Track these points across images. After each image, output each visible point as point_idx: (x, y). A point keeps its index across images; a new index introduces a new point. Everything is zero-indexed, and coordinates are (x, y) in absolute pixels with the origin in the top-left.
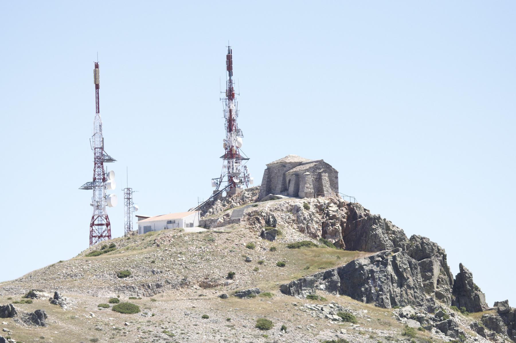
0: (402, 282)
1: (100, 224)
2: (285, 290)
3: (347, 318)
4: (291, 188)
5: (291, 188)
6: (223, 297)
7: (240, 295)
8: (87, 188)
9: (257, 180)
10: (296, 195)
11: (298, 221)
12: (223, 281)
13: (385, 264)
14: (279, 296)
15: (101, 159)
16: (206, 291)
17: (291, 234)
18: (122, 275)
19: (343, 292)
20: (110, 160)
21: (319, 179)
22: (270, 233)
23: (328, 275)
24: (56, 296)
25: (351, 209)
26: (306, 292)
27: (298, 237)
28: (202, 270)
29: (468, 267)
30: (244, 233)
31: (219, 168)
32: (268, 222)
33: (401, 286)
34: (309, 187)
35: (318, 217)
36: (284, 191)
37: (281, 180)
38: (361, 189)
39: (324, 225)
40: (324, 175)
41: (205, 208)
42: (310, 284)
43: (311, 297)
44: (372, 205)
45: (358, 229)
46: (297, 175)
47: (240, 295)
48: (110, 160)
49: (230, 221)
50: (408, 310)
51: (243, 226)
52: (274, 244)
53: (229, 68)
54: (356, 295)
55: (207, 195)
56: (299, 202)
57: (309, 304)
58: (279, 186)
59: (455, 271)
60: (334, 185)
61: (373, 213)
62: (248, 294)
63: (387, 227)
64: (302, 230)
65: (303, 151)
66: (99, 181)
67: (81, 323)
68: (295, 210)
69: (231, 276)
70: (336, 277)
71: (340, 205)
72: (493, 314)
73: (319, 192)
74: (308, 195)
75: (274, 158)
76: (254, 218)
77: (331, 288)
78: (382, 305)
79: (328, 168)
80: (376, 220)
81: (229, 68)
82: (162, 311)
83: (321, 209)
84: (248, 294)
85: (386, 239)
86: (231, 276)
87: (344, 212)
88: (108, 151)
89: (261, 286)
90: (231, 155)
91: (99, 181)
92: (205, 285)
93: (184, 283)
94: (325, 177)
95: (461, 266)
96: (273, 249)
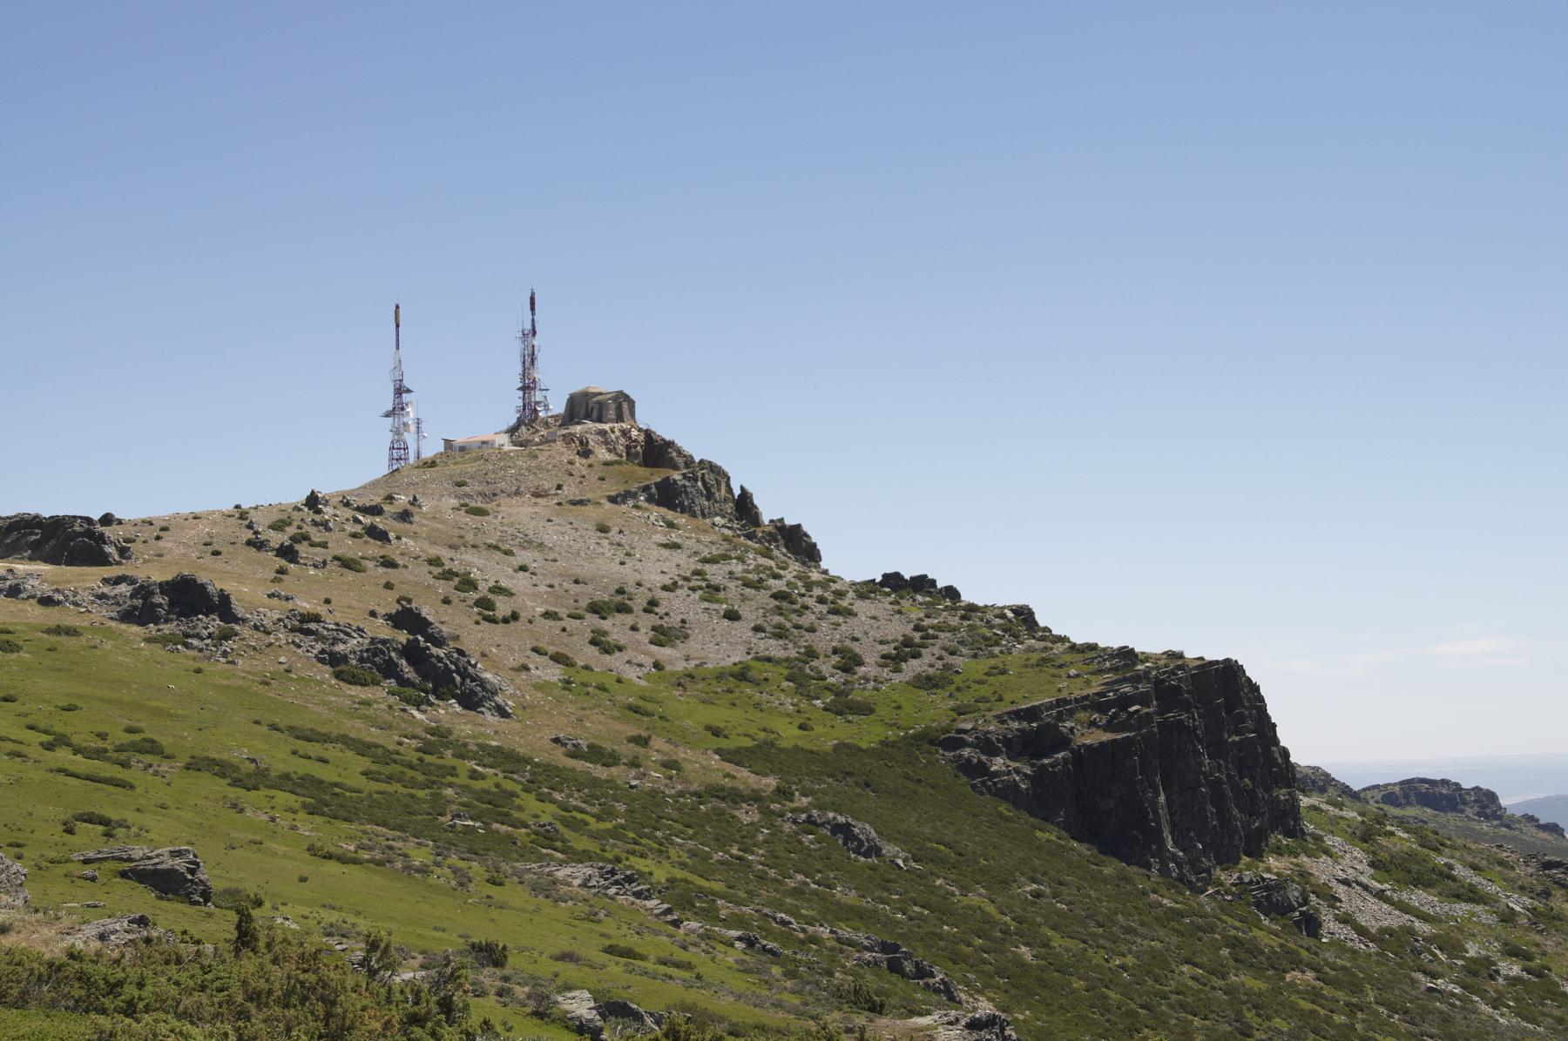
0: (710, 496)
1: (398, 449)
2: (612, 500)
3: (671, 525)
4: (595, 414)
5: (595, 414)
6: (559, 504)
7: (574, 503)
8: (387, 416)
9: (558, 406)
10: (600, 420)
11: (606, 443)
12: (553, 491)
13: (696, 480)
14: (608, 505)
15: (400, 391)
16: (539, 500)
17: (603, 454)
18: (460, 484)
19: (659, 504)
20: (408, 391)
21: (619, 408)
22: (586, 453)
23: (646, 489)
24: (415, 499)
25: (648, 434)
26: (631, 502)
27: (609, 457)
28: (531, 482)
29: (749, 489)
30: (562, 453)
31: (516, 400)
32: (581, 442)
33: (708, 499)
34: (612, 414)
35: (622, 441)
36: (588, 416)
37: (583, 407)
38: (653, 417)
39: (628, 447)
40: (623, 404)
41: (512, 431)
42: (634, 496)
43: (636, 507)
44: (664, 432)
45: (656, 451)
46: (600, 403)
47: (574, 503)
48: (408, 391)
49: (546, 441)
50: (718, 519)
51: (559, 445)
52: (590, 461)
53: (533, 308)
54: (672, 507)
55: (513, 421)
56: (606, 427)
57: (635, 512)
58: (583, 413)
59: (737, 492)
60: (632, 414)
61: (668, 438)
62: (581, 503)
63: (679, 452)
64: (610, 451)
65: (604, 383)
66: (397, 410)
67: (443, 522)
68: (603, 433)
69: (559, 487)
70: (654, 490)
71: (640, 430)
72: (771, 529)
73: (620, 419)
74: (611, 421)
75: (577, 387)
76: (568, 439)
77: (650, 500)
78: (694, 515)
79: (627, 398)
80: (671, 444)
81: (533, 308)
82: (510, 515)
83: (624, 433)
84: (581, 503)
85: (680, 461)
86: (559, 487)
87: (642, 438)
88: (407, 384)
89: (589, 496)
90: (527, 388)
91: (397, 410)
92: (537, 495)
93: (517, 493)
94: (625, 406)
95: (742, 488)
96: (590, 466)
